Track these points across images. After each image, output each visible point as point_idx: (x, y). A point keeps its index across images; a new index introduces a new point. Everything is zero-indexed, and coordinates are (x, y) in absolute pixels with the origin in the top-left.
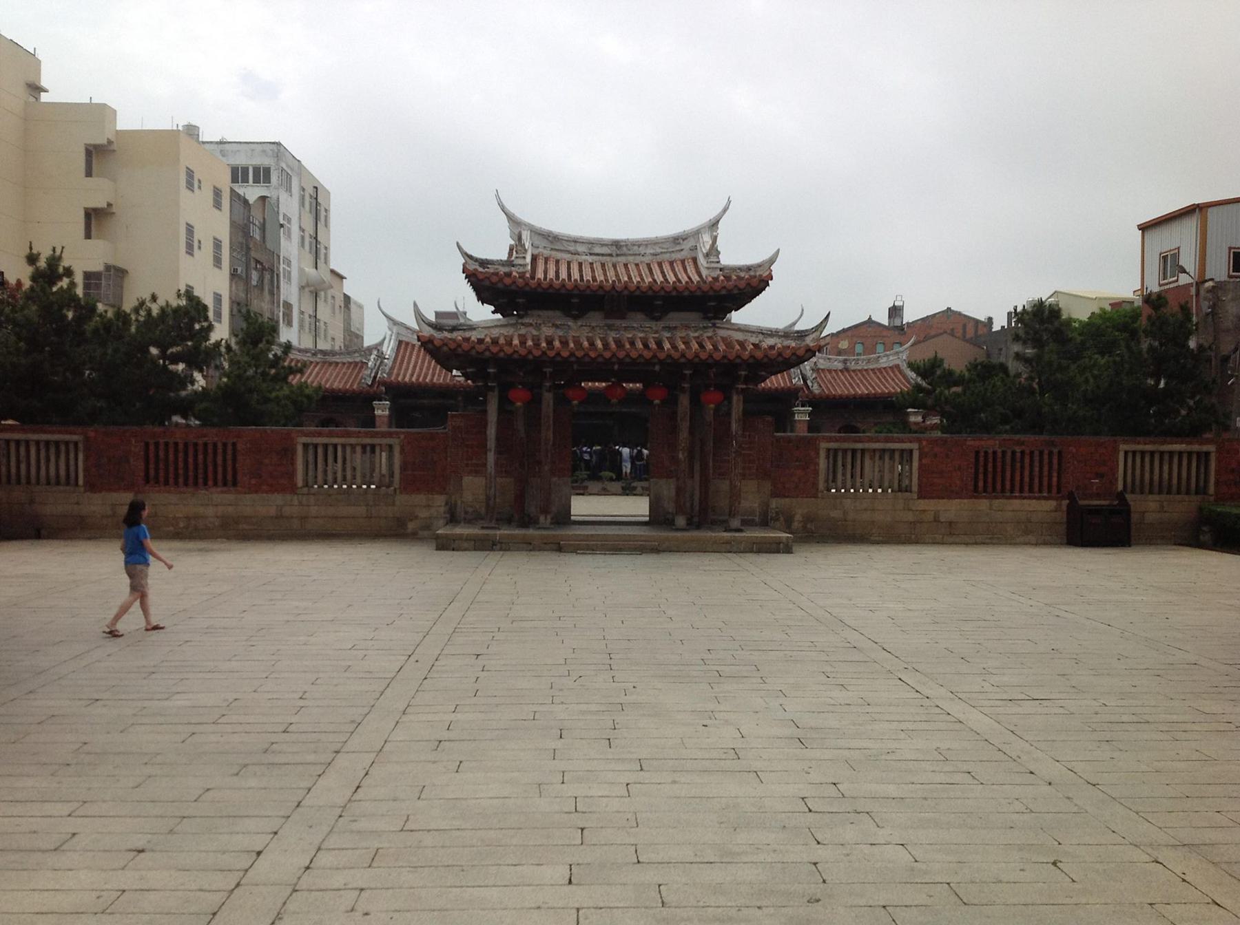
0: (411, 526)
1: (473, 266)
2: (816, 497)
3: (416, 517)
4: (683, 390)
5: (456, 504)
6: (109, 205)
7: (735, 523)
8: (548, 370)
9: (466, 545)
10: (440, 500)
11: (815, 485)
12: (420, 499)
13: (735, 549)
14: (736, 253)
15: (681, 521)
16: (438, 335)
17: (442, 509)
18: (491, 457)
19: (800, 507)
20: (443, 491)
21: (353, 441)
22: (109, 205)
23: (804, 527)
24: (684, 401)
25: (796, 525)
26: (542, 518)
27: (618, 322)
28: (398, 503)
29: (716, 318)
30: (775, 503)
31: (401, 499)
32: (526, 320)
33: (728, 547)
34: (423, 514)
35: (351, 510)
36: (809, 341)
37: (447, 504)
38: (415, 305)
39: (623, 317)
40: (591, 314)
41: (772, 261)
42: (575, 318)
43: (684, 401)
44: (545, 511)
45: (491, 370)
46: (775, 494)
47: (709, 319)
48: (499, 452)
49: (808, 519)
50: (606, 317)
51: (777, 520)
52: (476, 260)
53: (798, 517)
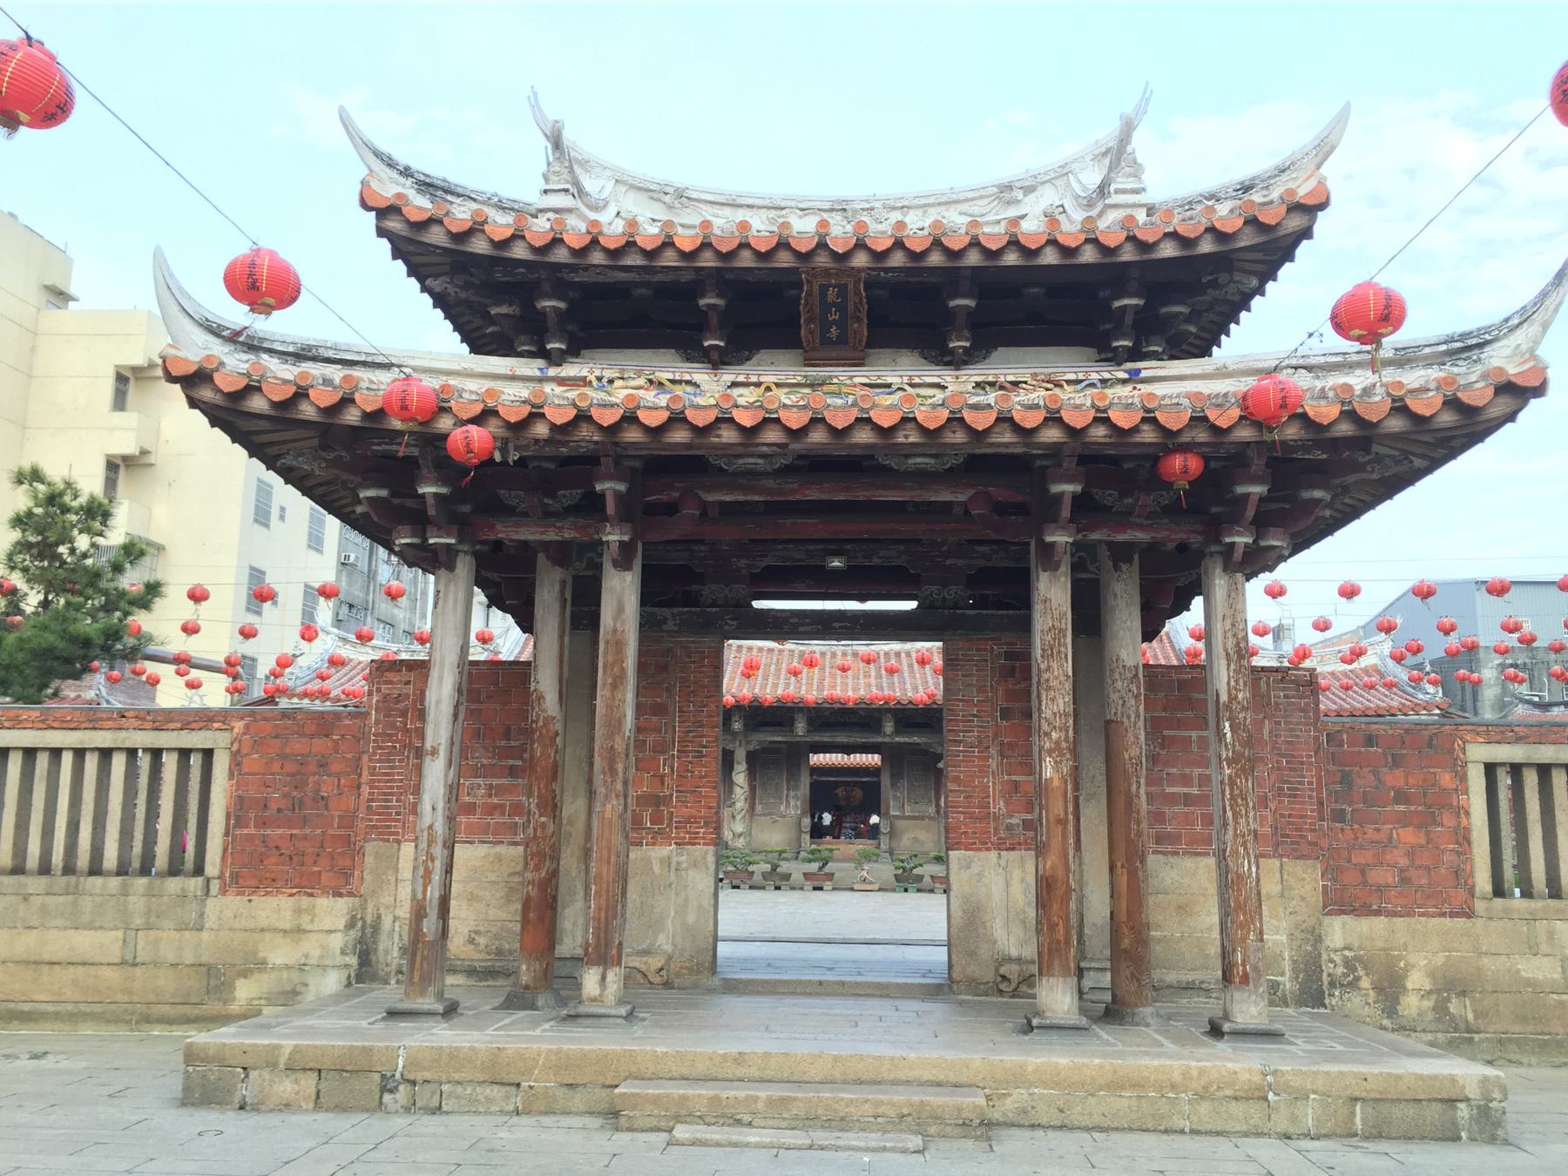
0: (245, 991)
1: (389, 188)
2: (1469, 914)
3: (262, 965)
4: (1050, 564)
5: (376, 927)
6: (144, 452)
7: (1249, 1010)
8: (609, 487)
9: (286, 1087)
10: (332, 912)
11: (1461, 876)
12: (275, 908)
13: (1281, 1123)
14: (1186, 173)
15: (1058, 998)
16: (234, 365)
17: (337, 941)
18: (436, 775)
19: (1422, 947)
20: (343, 881)
21: (103, 739)
22: (144, 452)
23: (1441, 1009)
24: (1053, 596)
25: (1412, 1004)
26: (590, 981)
27: (841, 374)
28: (211, 919)
29: (1136, 354)
30: (1340, 932)
31: (225, 909)
32: (570, 370)
33: (1255, 1113)
34: (279, 954)
35: (85, 942)
36: (1473, 380)
37: (351, 925)
38: (159, 261)
39: (859, 362)
40: (763, 355)
41: (1324, 149)
42: (716, 361)
43: (1053, 596)
44: (603, 953)
45: (427, 489)
46: (1339, 902)
47: (1115, 358)
48: (462, 756)
49: (1449, 985)
50: (809, 362)
51: (1354, 985)
52: (406, 172)
53: (1416, 980)
